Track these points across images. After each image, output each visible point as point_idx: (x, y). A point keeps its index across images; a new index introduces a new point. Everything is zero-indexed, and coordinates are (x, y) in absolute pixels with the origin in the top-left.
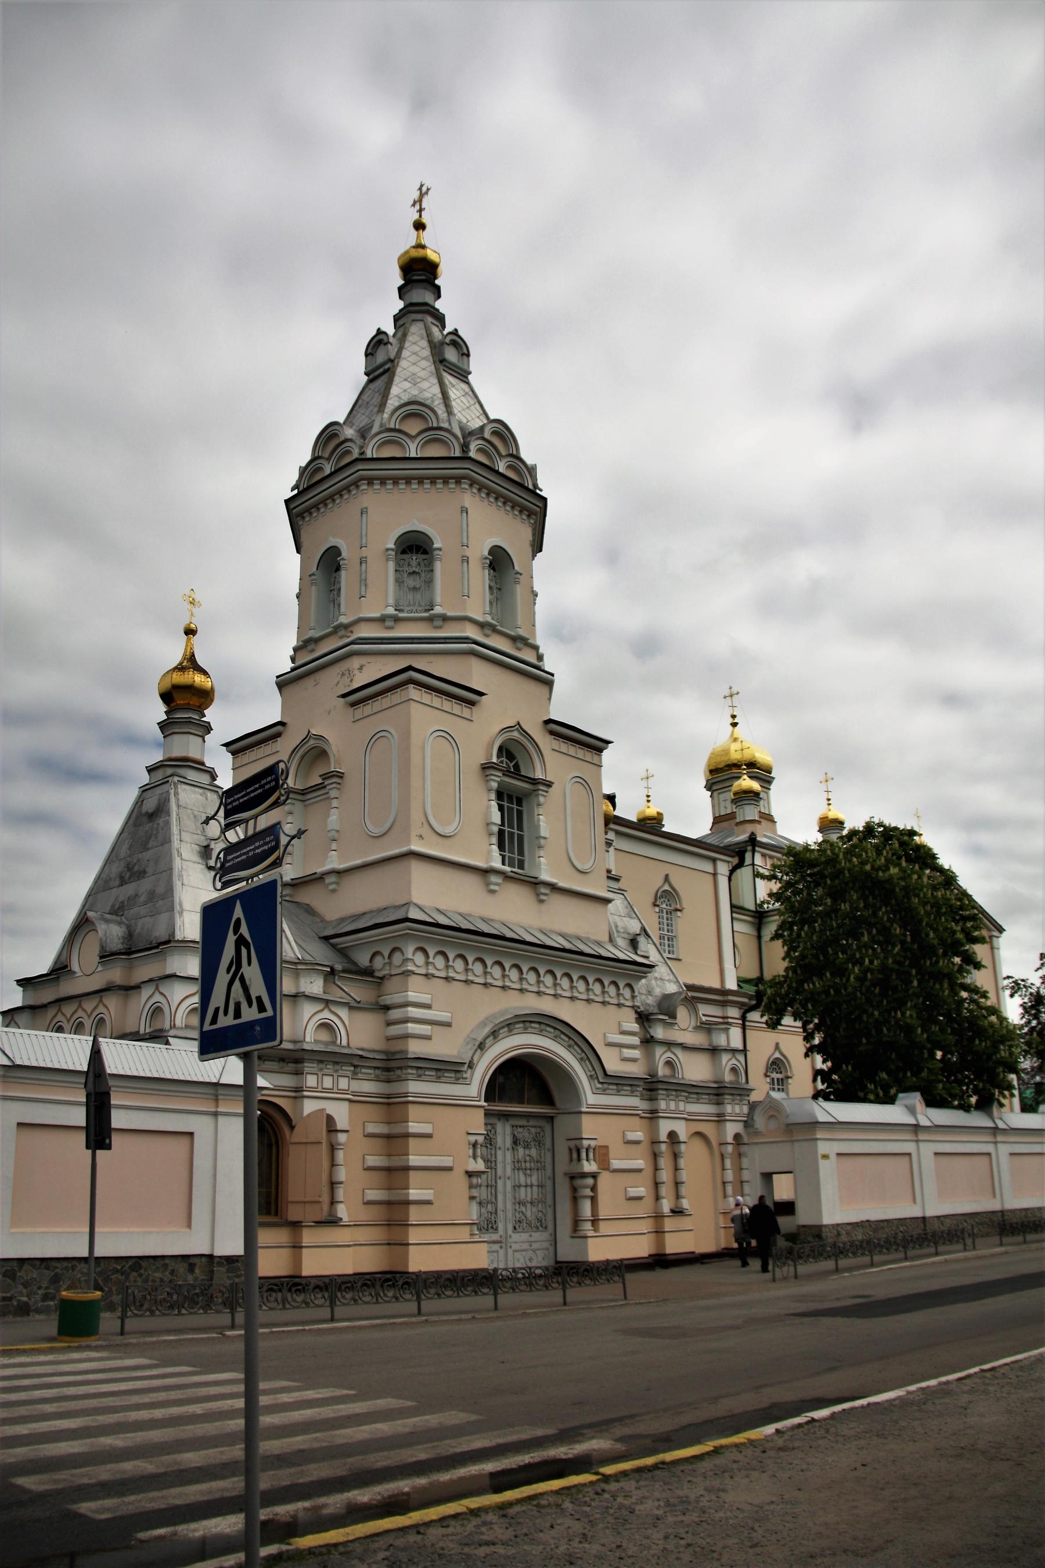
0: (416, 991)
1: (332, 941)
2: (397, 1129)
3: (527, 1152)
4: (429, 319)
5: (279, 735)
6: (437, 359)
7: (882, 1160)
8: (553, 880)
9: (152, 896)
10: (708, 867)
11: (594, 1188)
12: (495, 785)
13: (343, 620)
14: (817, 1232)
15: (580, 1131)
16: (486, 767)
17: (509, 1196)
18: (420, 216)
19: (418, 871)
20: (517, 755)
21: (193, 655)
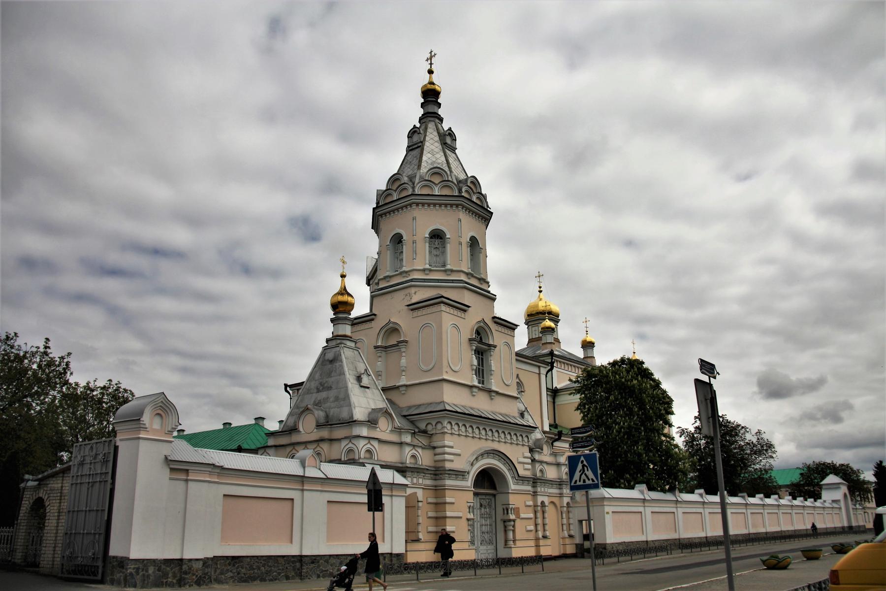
0: (448, 441)
1: (408, 417)
2: (440, 500)
3: (485, 510)
4: (437, 121)
5: (373, 320)
6: (442, 143)
7: (631, 515)
8: (498, 390)
9: (337, 399)
10: (536, 370)
11: (514, 526)
12: (474, 348)
13: (404, 269)
14: (604, 546)
15: (509, 501)
16: (470, 340)
17: (479, 529)
18: (431, 67)
19: (446, 387)
20: (481, 333)
21: (345, 287)
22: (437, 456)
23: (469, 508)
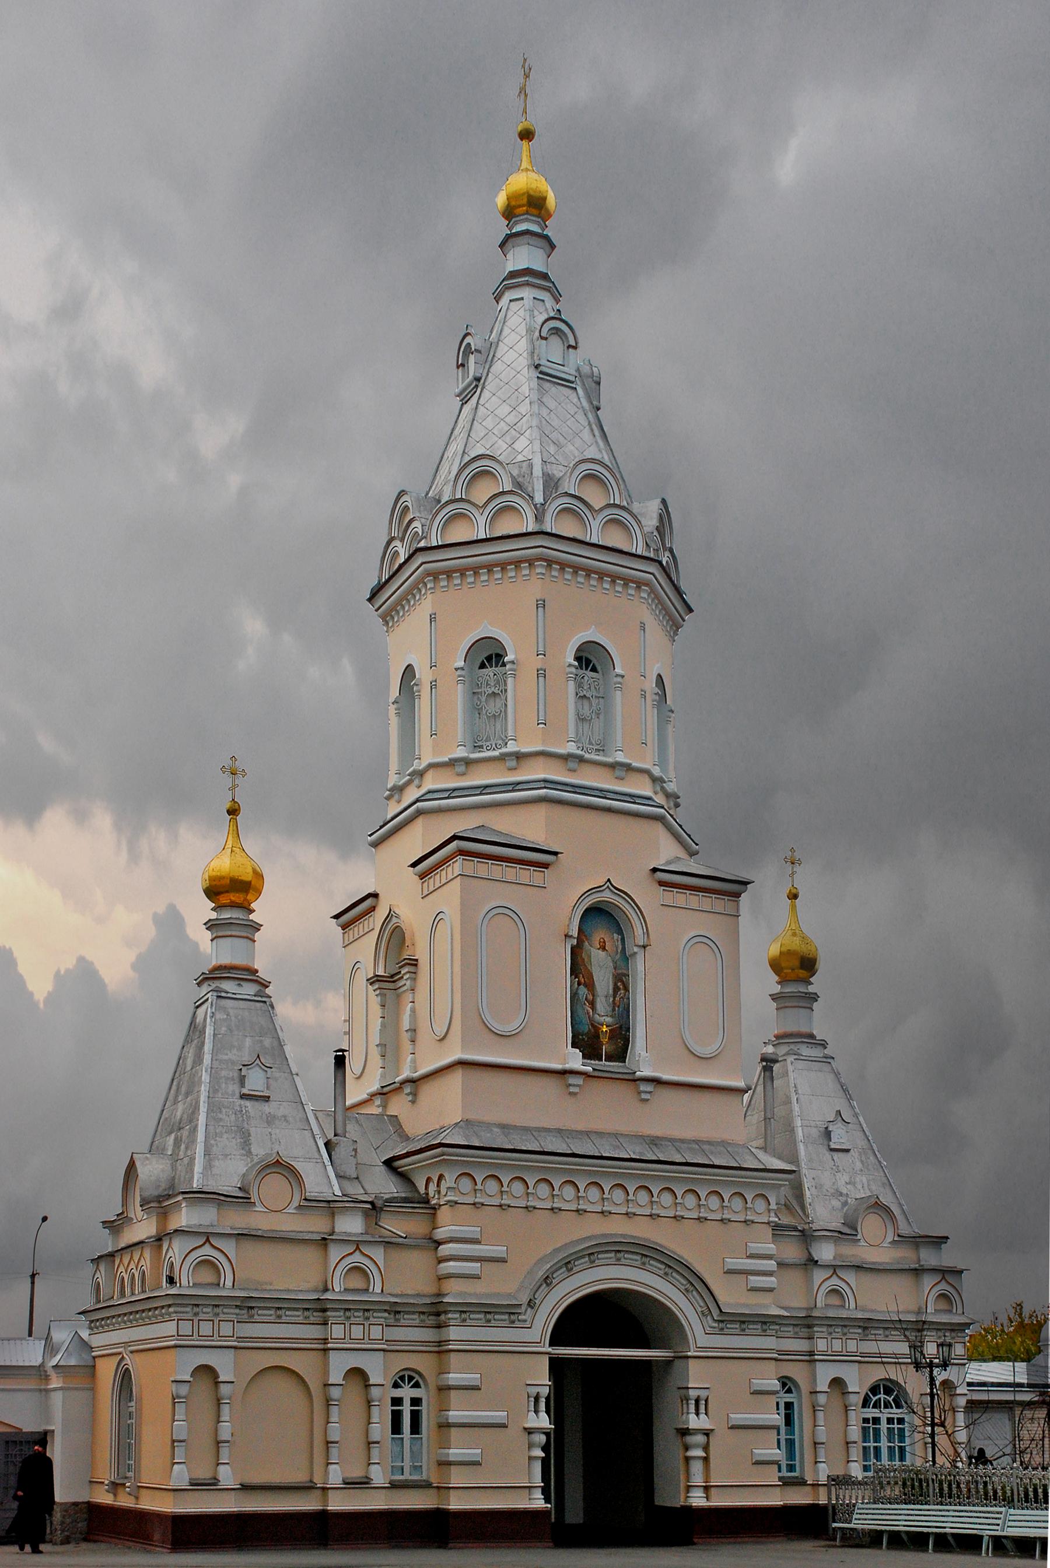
11: (706, 1448)
22: (442, 1265)
23: (537, 1399)
